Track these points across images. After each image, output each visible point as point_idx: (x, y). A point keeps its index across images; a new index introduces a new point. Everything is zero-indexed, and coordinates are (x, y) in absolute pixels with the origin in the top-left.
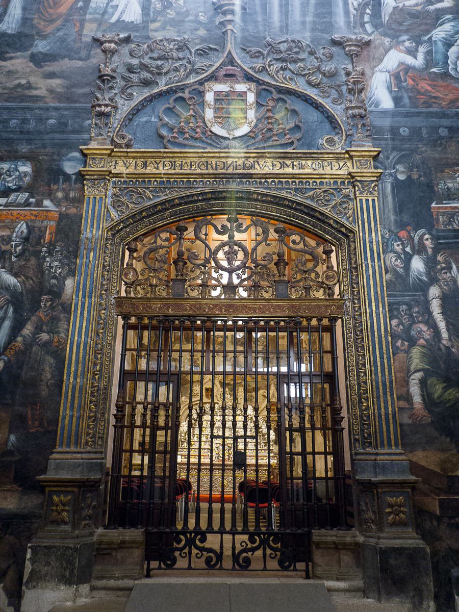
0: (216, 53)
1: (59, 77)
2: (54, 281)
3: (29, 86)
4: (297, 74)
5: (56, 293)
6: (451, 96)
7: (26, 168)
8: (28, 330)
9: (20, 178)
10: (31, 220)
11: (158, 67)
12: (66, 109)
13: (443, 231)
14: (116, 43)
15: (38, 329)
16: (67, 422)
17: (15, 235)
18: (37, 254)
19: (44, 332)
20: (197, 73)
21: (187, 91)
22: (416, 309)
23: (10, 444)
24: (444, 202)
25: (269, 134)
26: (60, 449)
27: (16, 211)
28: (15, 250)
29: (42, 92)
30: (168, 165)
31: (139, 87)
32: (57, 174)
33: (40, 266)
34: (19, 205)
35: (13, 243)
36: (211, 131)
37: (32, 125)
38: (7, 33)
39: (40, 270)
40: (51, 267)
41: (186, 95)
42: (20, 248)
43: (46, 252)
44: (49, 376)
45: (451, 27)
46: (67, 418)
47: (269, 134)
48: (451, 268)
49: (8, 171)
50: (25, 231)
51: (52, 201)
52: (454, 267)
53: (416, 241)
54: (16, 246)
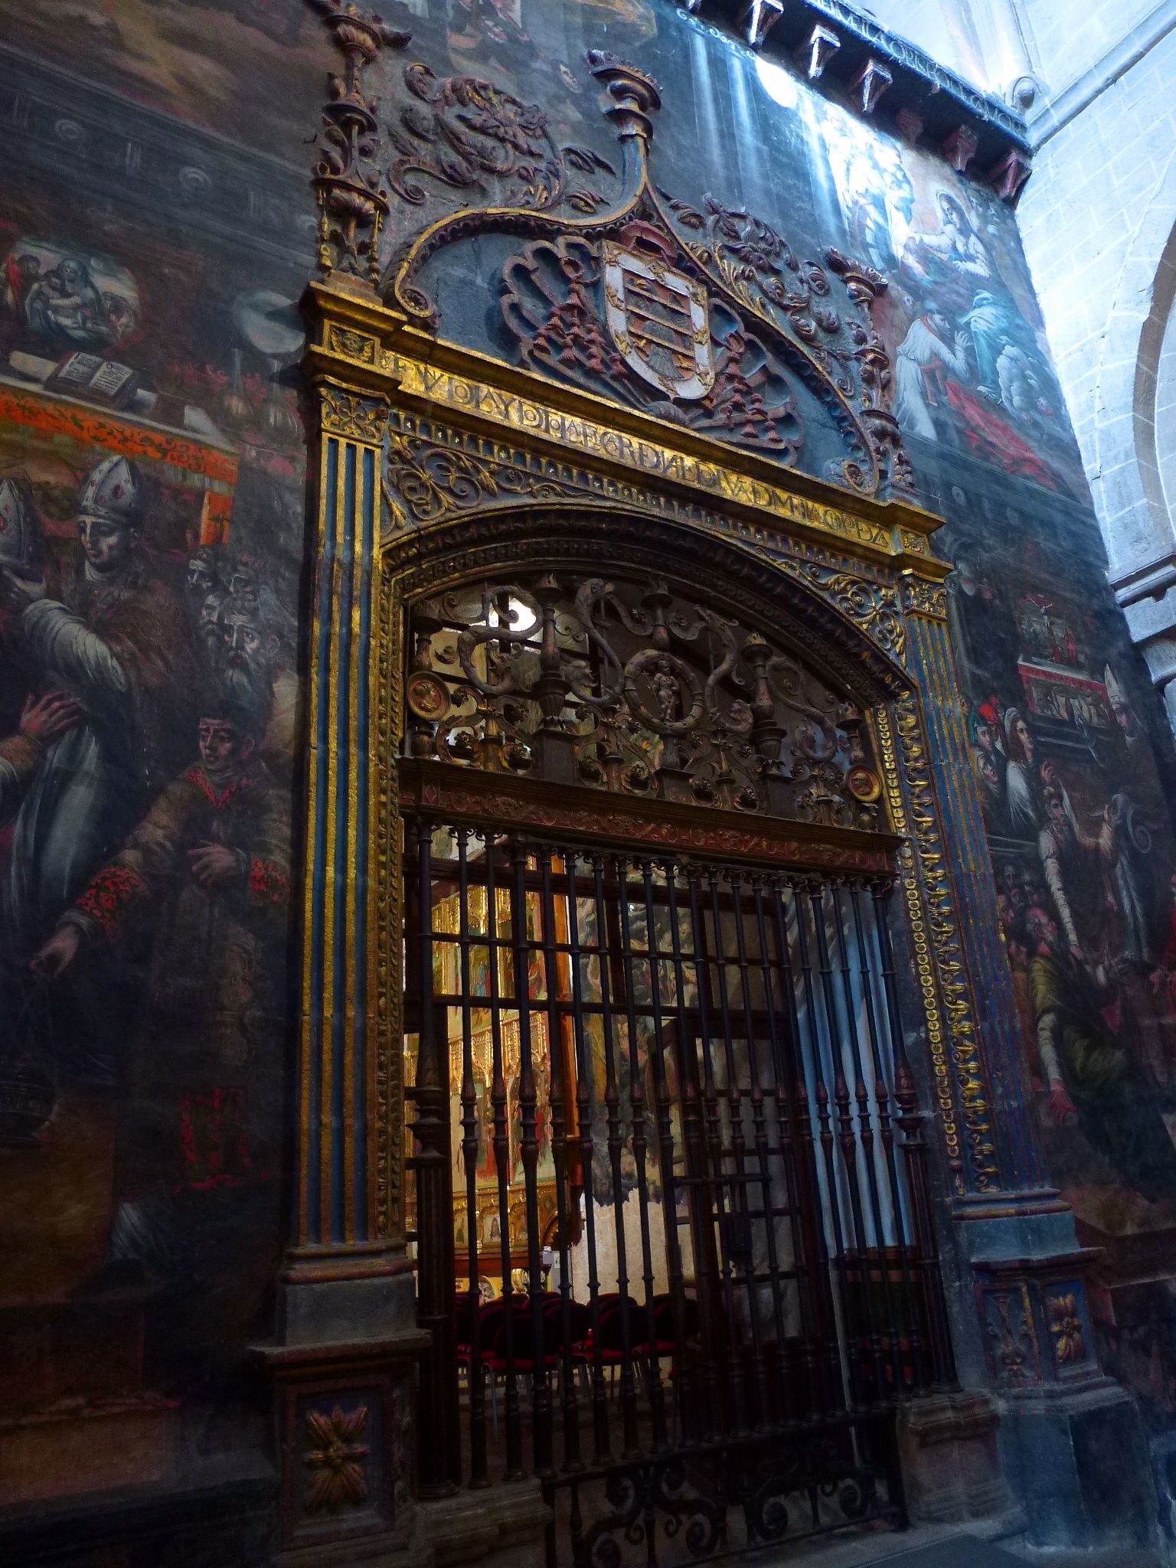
0: (609, 177)
1: (204, 52)
2: (235, 676)
4: (772, 300)
7: (120, 287)
11: (482, 153)
12: (244, 158)
14: (374, 36)
16: (327, 1152)
17: (90, 492)
19: (216, 840)
20: (575, 207)
21: (561, 240)
22: (1027, 877)
23: (121, 1240)
24: (1035, 659)
25: (737, 416)
26: (312, 1248)
28: (95, 543)
30: (530, 415)
31: (438, 183)
34: (98, 396)
35: (89, 520)
36: (624, 363)
39: (187, 629)
41: (560, 250)
42: (112, 540)
43: (202, 574)
44: (245, 996)
45: (993, 317)
46: (327, 1140)
47: (737, 416)
48: (1061, 798)
50: (129, 488)
53: (1008, 729)
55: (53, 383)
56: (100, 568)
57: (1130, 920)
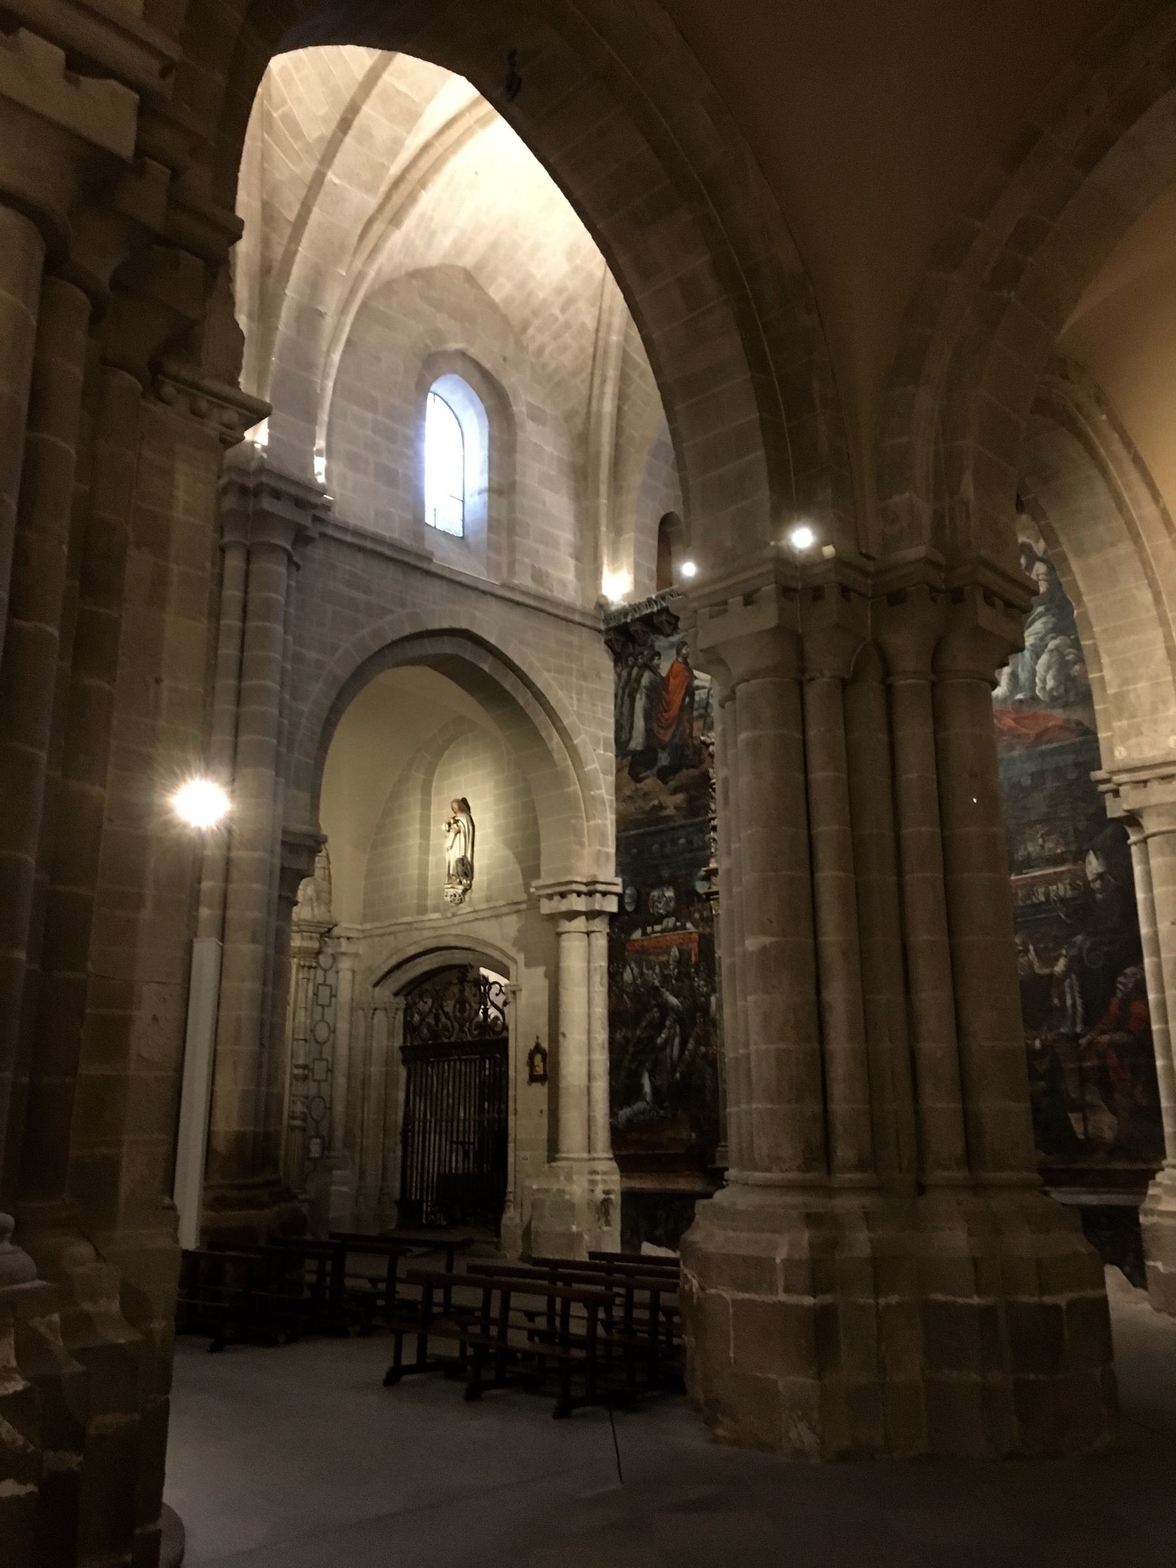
3: (661, 807)
5: (706, 1010)
7: (670, 893)
9: (667, 903)
10: (681, 944)
13: (1021, 908)
15: (698, 1043)
18: (688, 975)
24: (1024, 871)
27: (669, 936)
29: (670, 811)
33: (692, 986)
35: (671, 967)
37: (668, 849)
38: (637, 751)
39: (692, 989)
40: (699, 986)
48: (1028, 950)
49: (659, 898)
51: (692, 923)
52: (1031, 947)
54: (674, 969)
55: (662, 931)
56: (675, 979)
57: (1070, 1011)
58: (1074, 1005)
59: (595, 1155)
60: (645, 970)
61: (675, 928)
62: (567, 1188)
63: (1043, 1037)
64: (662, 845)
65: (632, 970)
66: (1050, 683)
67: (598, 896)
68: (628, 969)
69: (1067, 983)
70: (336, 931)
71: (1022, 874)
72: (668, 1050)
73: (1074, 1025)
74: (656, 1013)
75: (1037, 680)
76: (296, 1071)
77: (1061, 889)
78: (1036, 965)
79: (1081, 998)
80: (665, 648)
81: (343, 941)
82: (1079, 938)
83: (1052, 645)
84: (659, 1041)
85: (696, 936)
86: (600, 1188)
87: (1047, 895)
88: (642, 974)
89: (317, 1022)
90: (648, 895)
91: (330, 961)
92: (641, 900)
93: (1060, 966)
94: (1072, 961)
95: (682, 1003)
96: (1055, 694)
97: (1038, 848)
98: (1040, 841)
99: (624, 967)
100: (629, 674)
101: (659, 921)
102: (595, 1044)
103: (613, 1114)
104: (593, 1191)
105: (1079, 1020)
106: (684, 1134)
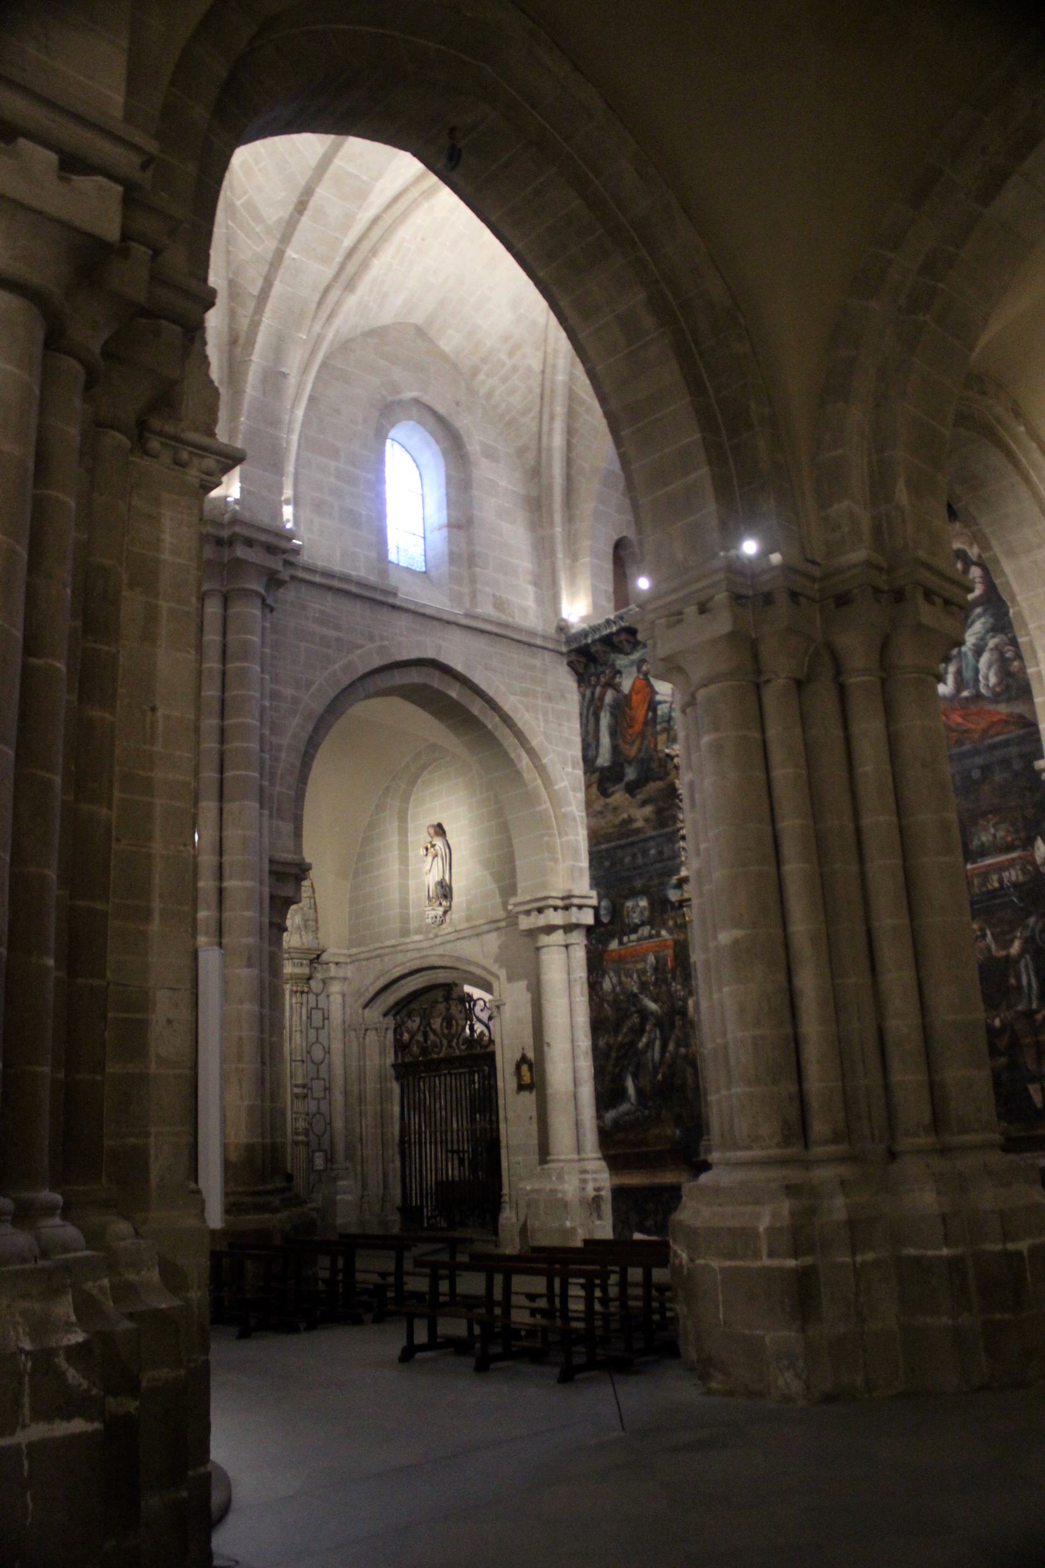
3: (630, 820)
5: (683, 1012)
6: (983, 724)
7: (643, 903)
8: (671, 1047)
9: (642, 913)
15: (678, 1045)
18: (665, 981)
24: (979, 860)
27: (646, 944)
29: (639, 824)
32: (665, 902)
33: (669, 991)
35: (649, 974)
37: (640, 861)
39: (671, 995)
49: (633, 908)
52: (988, 932)
54: (651, 976)
55: (639, 940)
56: (653, 985)
57: (1026, 990)
58: (1029, 984)
59: (584, 1156)
60: (624, 979)
61: (651, 937)
62: (560, 1187)
63: (1002, 1016)
64: (634, 856)
65: (611, 979)
66: (993, 680)
67: (574, 910)
68: (607, 979)
69: (1022, 964)
70: (325, 957)
71: (977, 862)
72: (649, 1054)
73: (1030, 1001)
74: (636, 1019)
75: (981, 678)
76: (296, 1090)
77: (1013, 875)
78: (993, 947)
79: (1035, 976)
80: (625, 667)
81: (332, 967)
82: (1032, 920)
83: (992, 643)
84: (640, 1045)
85: (671, 943)
86: (590, 1187)
87: (1001, 881)
88: (620, 982)
89: (313, 1044)
90: (623, 905)
91: (321, 985)
92: (616, 911)
93: (1016, 948)
94: (1029, 943)
95: (661, 1007)
96: (998, 689)
97: (990, 838)
98: (992, 830)
99: (603, 976)
100: (593, 693)
101: (635, 929)
102: (578, 1052)
103: (599, 1116)
104: (584, 1189)
105: (1034, 998)
106: (669, 1132)
